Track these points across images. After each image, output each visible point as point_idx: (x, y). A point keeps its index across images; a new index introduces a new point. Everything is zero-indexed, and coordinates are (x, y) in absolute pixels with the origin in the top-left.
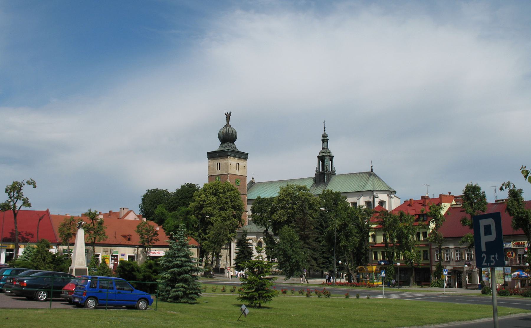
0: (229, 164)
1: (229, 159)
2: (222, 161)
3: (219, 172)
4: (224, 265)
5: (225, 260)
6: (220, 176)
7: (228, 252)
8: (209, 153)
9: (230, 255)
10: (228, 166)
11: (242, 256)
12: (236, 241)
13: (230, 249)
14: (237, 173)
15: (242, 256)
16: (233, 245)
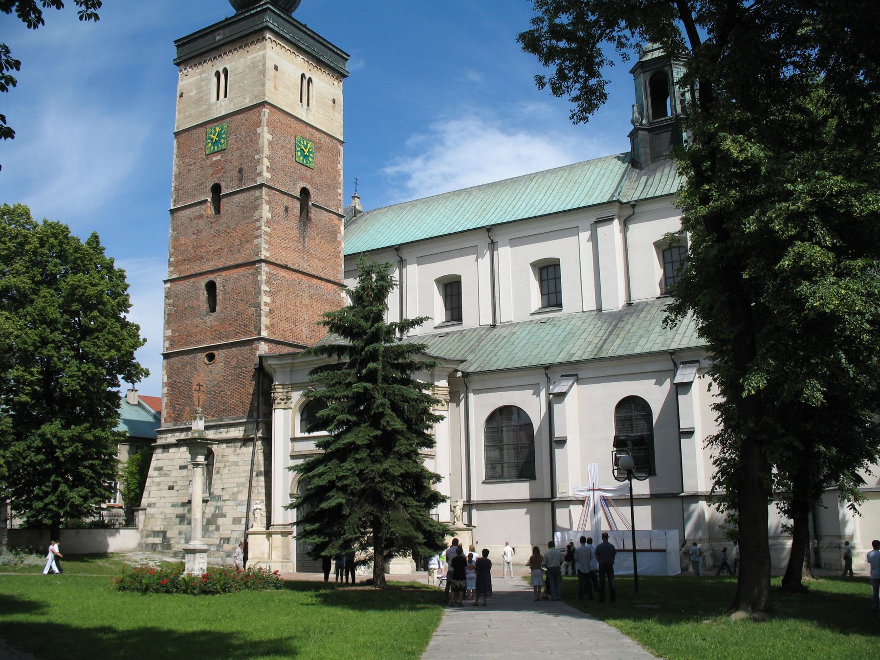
0: (270, 65)
1: (268, 44)
2: (237, 62)
3: (224, 107)
4: (236, 521)
5: (244, 497)
6: (225, 124)
7: (260, 458)
8: (181, 44)
9: (268, 474)
10: (263, 72)
11: (363, 435)
12: (297, 397)
13: (267, 441)
14: (300, 112)
15: (363, 435)
16: (286, 421)
